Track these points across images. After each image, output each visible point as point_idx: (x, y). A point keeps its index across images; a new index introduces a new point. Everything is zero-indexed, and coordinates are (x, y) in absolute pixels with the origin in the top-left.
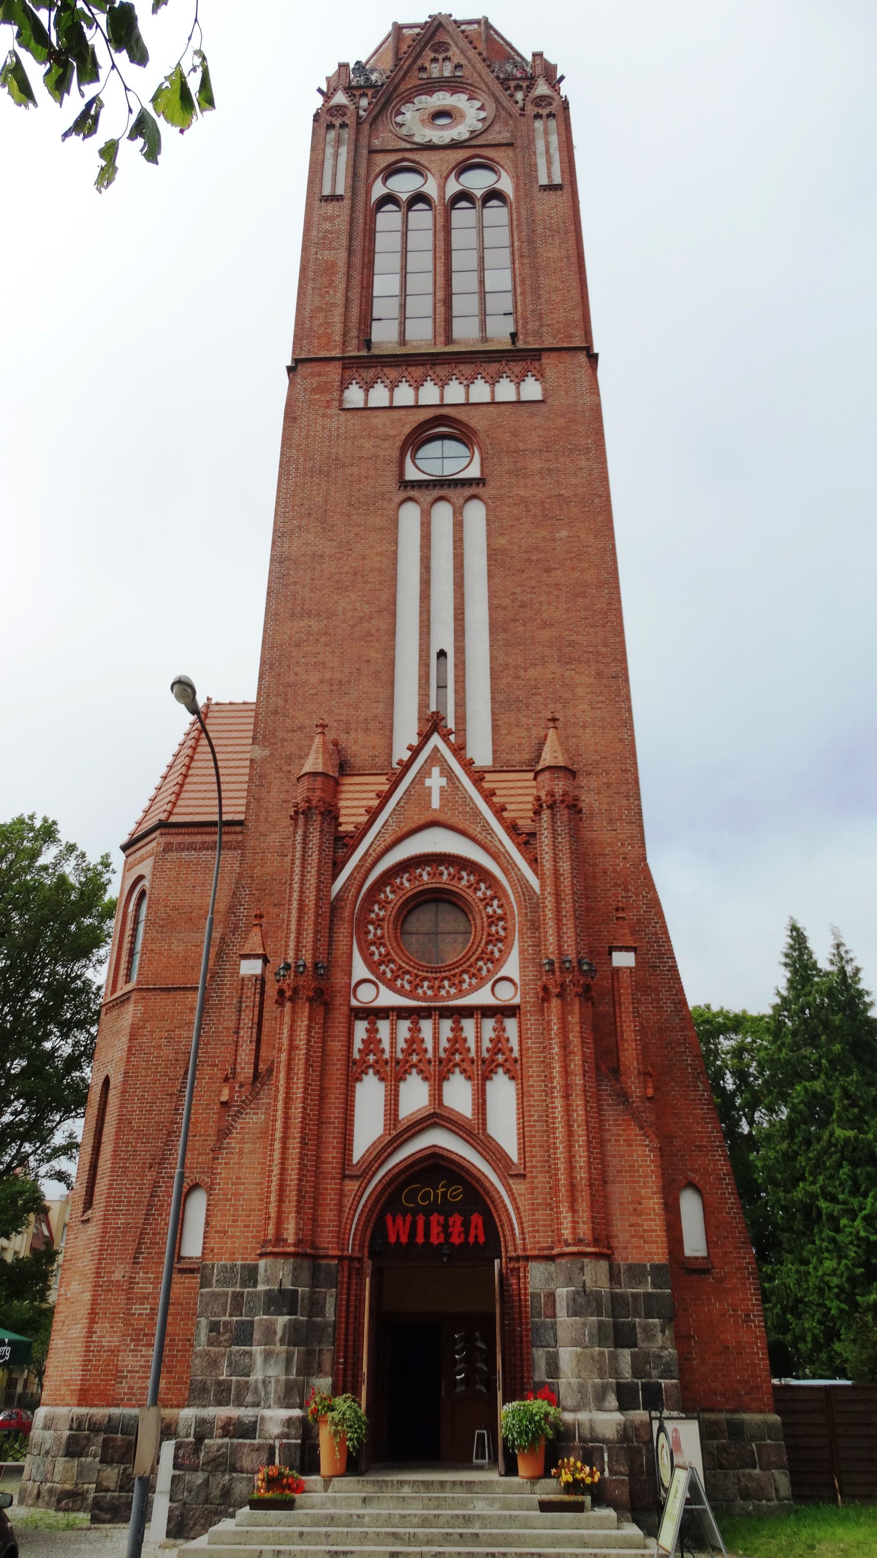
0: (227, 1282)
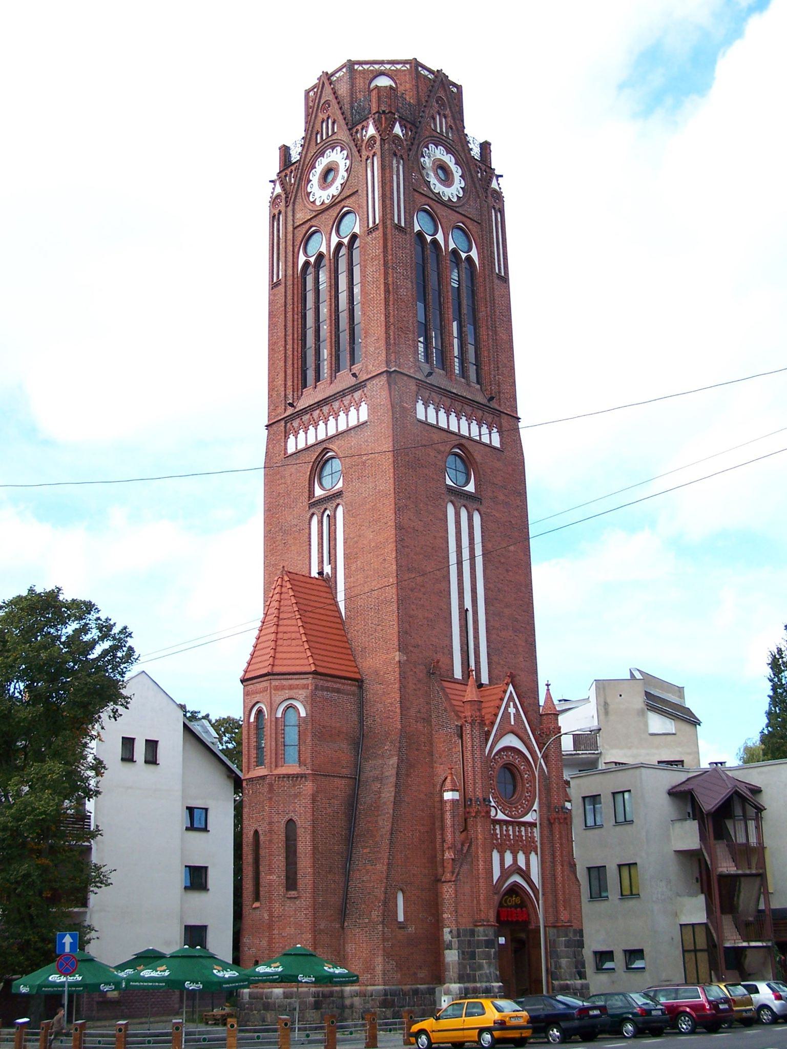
0: (465, 936)
